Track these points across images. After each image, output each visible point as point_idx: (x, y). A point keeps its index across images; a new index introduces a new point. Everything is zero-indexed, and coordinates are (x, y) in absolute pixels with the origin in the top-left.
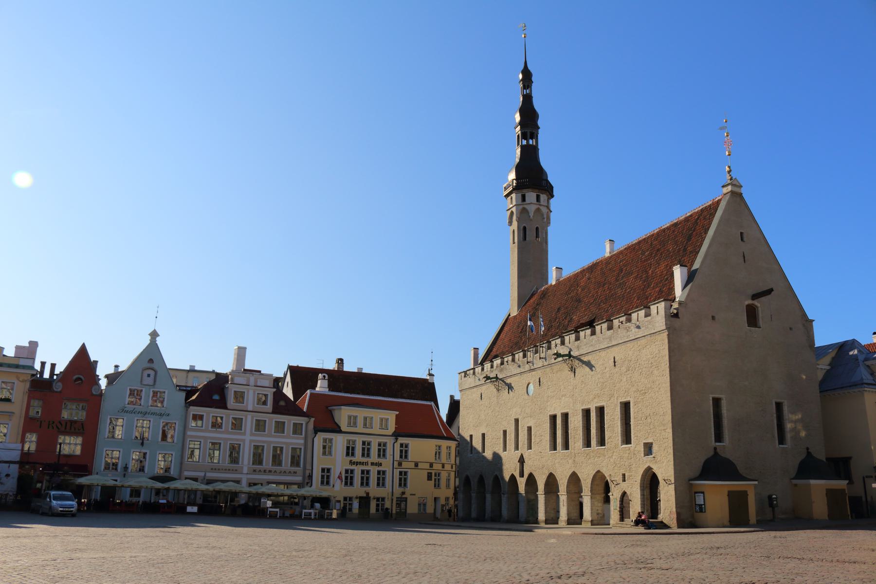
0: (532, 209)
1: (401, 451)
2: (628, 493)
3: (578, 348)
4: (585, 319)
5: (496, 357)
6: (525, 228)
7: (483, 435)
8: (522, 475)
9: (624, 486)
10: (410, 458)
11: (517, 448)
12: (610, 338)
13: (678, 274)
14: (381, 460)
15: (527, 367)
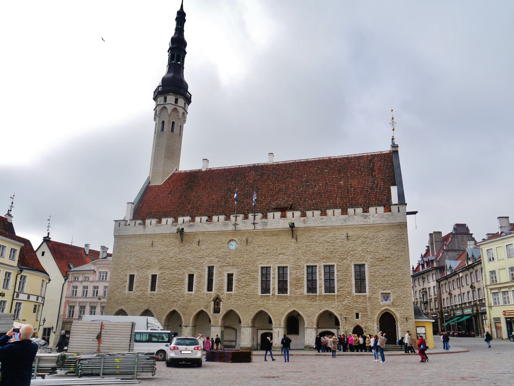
0: (181, 111)
1: (20, 282)
2: (362, 326)
3: (304, 221)
4: (282, 203)
5: (183, 215)
6: (173, 123)
7: (154, 277)
8: (217, 310)
9: (358, 322)
10: (25, 290)
11: (210, 288)
12: (345, 220)
13: (394, 190)
14: (5, 291)
15: (231, 228)
